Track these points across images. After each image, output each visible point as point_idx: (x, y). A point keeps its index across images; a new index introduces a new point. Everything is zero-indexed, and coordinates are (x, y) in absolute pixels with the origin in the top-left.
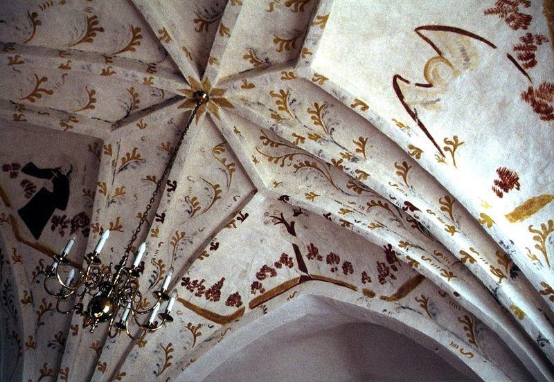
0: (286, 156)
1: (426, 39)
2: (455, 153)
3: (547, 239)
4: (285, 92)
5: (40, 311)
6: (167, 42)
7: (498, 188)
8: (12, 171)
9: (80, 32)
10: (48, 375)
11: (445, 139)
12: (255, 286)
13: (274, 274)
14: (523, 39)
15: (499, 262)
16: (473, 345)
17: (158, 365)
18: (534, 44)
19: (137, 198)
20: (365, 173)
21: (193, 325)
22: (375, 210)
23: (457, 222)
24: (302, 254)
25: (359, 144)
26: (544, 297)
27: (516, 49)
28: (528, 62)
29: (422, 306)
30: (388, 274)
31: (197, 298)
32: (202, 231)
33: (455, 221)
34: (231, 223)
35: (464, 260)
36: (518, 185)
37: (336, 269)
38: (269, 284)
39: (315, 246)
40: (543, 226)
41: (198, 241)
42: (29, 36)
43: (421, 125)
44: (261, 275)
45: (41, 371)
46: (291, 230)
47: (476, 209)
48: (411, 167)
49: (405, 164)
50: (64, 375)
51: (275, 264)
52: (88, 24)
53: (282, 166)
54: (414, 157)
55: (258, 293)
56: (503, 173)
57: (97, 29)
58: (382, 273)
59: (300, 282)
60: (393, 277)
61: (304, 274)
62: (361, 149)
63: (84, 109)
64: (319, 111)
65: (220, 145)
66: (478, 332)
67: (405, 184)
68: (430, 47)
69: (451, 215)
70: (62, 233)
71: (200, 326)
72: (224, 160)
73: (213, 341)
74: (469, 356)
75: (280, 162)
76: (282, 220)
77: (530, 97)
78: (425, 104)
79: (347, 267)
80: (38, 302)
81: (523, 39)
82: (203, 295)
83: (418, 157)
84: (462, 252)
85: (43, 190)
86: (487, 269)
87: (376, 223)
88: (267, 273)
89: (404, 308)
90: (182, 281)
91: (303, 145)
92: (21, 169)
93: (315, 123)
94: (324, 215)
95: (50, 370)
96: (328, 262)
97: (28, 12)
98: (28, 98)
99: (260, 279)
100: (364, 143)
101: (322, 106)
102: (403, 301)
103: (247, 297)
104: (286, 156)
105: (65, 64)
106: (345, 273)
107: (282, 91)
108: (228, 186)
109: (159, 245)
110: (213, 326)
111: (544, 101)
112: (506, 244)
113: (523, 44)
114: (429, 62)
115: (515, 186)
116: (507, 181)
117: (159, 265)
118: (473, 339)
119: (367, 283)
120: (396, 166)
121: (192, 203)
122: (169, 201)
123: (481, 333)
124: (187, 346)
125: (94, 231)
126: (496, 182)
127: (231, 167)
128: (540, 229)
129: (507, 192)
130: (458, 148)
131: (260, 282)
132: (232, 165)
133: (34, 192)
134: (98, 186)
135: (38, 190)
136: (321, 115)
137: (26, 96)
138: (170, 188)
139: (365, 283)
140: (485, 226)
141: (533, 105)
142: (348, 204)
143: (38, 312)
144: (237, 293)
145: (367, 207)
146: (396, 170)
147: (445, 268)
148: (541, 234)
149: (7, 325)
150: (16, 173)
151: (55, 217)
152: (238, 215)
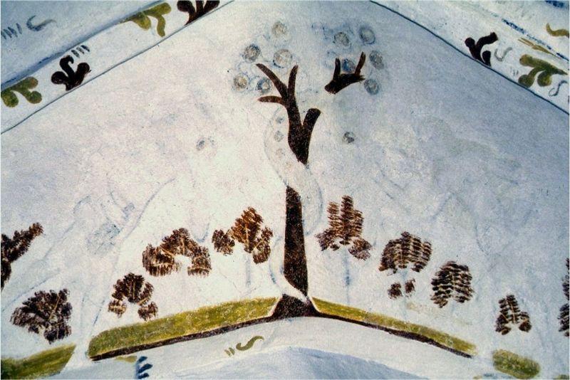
12: (130, 288)
13: (201, 265)
24: (306, 229)
32: (38, 28)
37: (410, 287)
39: (356, 206)
44: (159, 259)
46: (300, 143)
51: (215, 236)
55: (131, 315)
59: (277, 316)
61: (295, 293)
76: (287, 96)
88: (179, 258)
96: (387, 264)
99: (153, 270)
106: (440, 299)
139: (506, 331)
144: (63, 294)
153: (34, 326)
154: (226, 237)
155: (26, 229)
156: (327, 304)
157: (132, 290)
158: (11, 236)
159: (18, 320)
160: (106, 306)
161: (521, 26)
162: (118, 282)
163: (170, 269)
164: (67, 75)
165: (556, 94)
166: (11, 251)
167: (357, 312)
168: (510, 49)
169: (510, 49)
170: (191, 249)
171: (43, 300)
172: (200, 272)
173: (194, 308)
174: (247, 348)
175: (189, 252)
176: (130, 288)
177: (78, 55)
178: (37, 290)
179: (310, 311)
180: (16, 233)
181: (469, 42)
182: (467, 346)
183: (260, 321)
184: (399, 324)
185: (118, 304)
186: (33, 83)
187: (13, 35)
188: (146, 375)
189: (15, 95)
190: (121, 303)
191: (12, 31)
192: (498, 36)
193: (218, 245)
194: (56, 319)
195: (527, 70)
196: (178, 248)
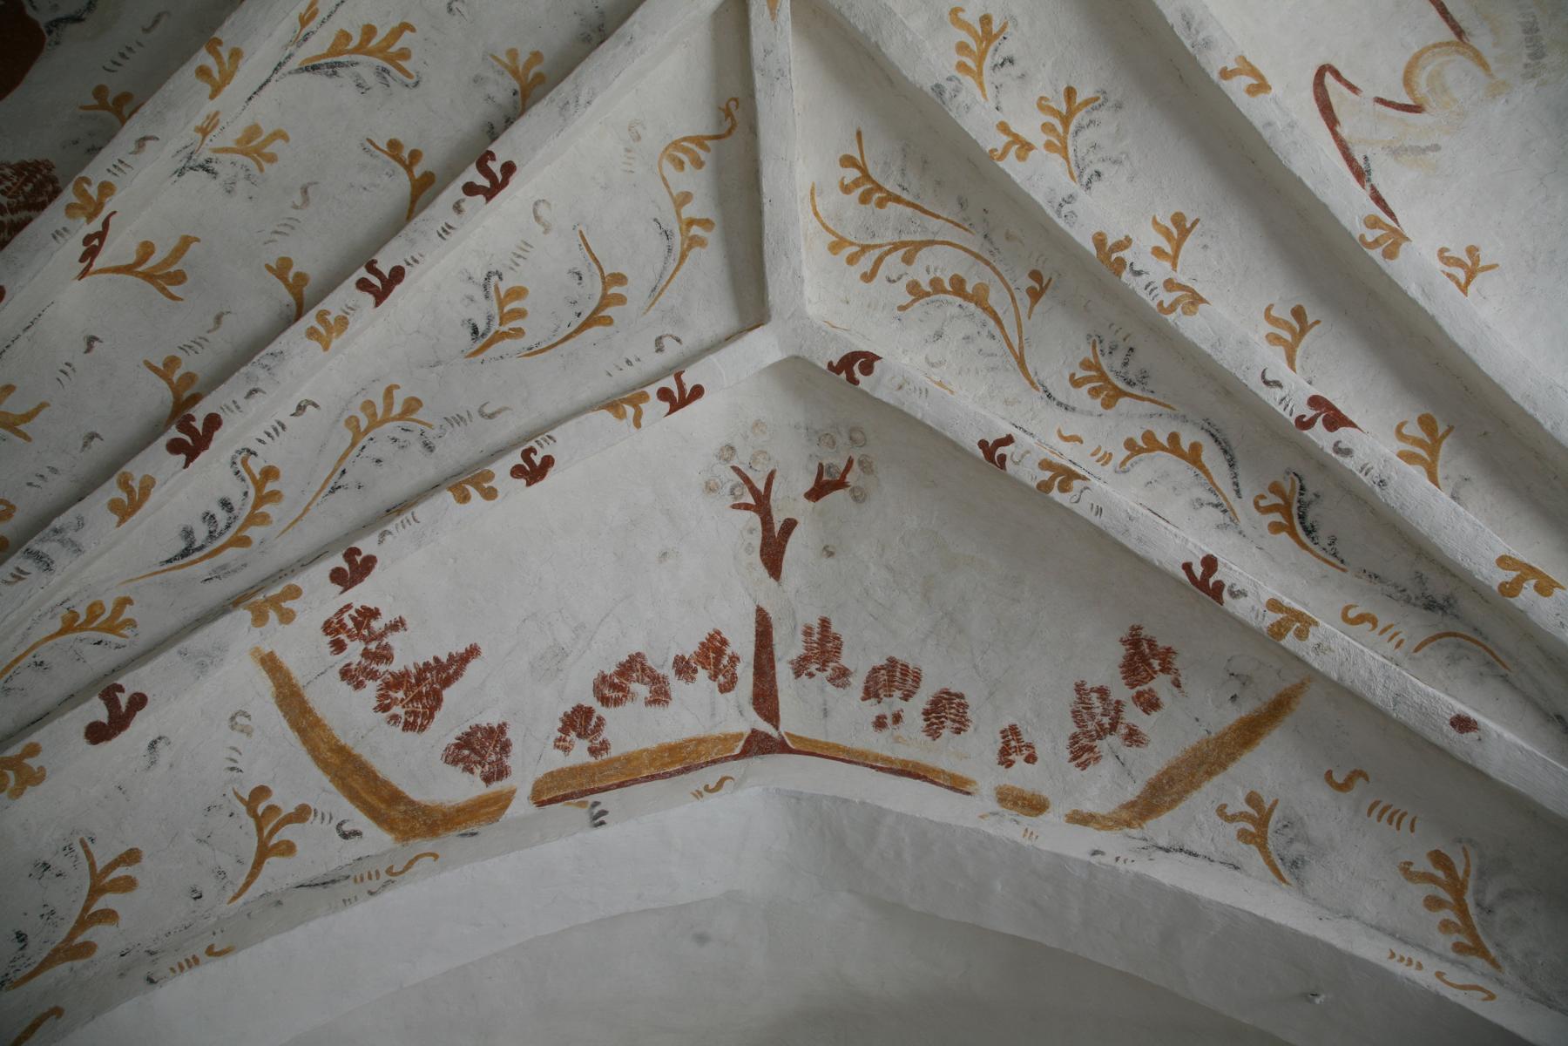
0: (896, 247)
4: (995, 29)
11: (1442, 251)
12: (579, 721)
13: (660, 696)
19: (306, 201)
20: (1193, 292)
21: (273, 800)
25: (1167, 234)
29: (1243, 836)
31: (345, 688)
32: (491, 416)
34: (629, 401)
35: (1510, 589)
37: (897, 718)
39: (835, 628)
41: (456, 450)
44: (612, 688)
46: (772, 557)
48: (1317, 322)
49: (1298, 313)
51: (676, 662)
53: (868, 277)
55: (580, 753)
58: (1091, 726)
59: (745, 753)
60: (1133, 737)
61: (765, 727)
62: (1168, 249)
65: (699, 141)
71: (302, 814)
72: (686, 198)
73: (348, 889)
75: (866, 263)
76: (762, 504)
78: (1396, 152)
82: (372, 687)
83: (1390, 254)
84: (1504, 562)
89: (1167, 851)
90: (339, 561)
91: (1020, 165)
94: (983, 444)
96: (870, 693)
99: (605, 701)
100: (1184, 233)
101: (1087, 103)
102: (1161, 827)
104: (896, 247)
106: (933, 731)
107: (986, 20)
108: (656, 292)
109: (301, 408)
110: (356, 833)
117: (259, 486)
120: (1268, 315)
121: (501, 306)
122: (447, 229)
124: (209, 887)
125: (70, 208)
127: (696, 230)
130: (1480, 277)
132: (706, 223)
134: (203, 52)
136: (1072, 128)
138: (483, 182)
139: (1010, 764)
142: (1055, 440)
144: (502, 728)
145: (1121, 453)
146: (1268, 328)
152: (670, 383)
153: (469, 766)
154: (687, 662)
155: (462, 650)
156: (801, 739)
157: (581, 725)
158: (444, 659)
159: (450, 758)
160: (551, 742)
161: (1030, 430)
162: (565, 714)
163: (624, 699)
164: (528, 468)
165: (1077, 502)
166: (444, 676)
167: (837, 747)
168: (1028, 452)
169: (1028, 452)
170: (648, 677)
171: (479, 735)
172: (659, 704)
173: (651, 744)
174: (717, 790)
175: (647, 679)
176: (578, 721)
177: (542, 446)
178: (473, 723)
179: (781, 747)
180: (451, 656)
181: (983, 444)
182: (966, 782)
183: (726, 759)
185: (564, 740)
186: (490, 476)
187: (461, 423)
188: (602, 823)
189: (467, 490)
190: (568, 738)
191: (461, 418)
192: (1014, 438)
193: (679, 672)
194: (493, 758)
195: (1047, 475)
196: (634, 675)
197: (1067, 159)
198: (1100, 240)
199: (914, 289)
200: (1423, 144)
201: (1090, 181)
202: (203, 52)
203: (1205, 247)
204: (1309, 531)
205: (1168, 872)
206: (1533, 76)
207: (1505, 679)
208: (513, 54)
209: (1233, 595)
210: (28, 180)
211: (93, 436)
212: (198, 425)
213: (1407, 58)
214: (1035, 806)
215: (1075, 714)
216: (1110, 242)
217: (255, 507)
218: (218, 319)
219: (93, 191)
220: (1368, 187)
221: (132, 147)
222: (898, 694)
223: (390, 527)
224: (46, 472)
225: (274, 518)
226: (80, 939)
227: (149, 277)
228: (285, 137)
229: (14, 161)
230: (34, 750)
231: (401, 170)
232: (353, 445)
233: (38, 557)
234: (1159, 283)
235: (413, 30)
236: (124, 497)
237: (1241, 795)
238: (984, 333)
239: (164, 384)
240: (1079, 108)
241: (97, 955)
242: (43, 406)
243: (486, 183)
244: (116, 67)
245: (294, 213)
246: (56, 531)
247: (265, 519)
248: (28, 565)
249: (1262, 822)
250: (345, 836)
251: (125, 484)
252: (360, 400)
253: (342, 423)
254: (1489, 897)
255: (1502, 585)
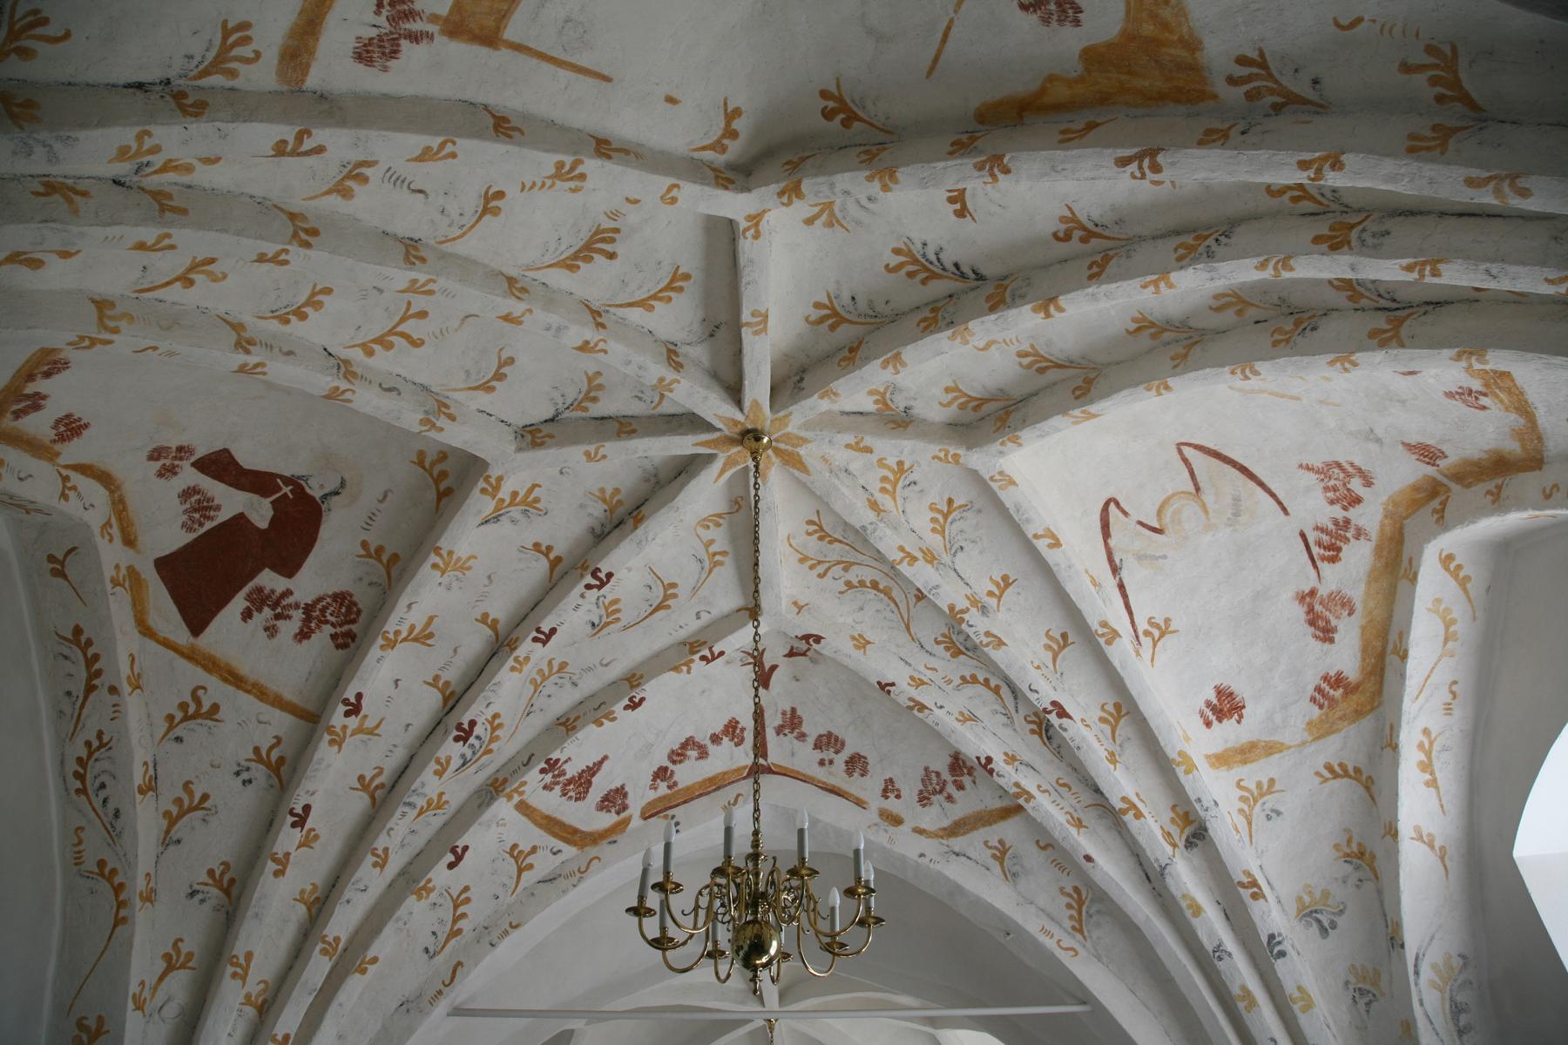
0: (839, 563)
1: (1185, 461)
2: (1160, 644)
3: (1259, 804)
4: (906, 466)
5: (175, 810)
6: (756, 333)
7: (1209, 714)
8: (168, 462)
9: (563, 248)
10: (183, 966)
11: (1150, 618)
12: (661, 774)
13: (703, 754)
14: (1336, 522)
15: (1173, 820)
16: (1078, 936)
17: (434, 933)
18: (1349, 535)
20: (1000, 639)
22: (970, 690)
23: (1120, 746)
24: (767, 722)
25: (998, 585)
26: (1242, 890)
27: (1317, 528)
28: (1327, 553)
29: (994, 856)
30: (941, 792)
32: (606, 665)
33: (1118, 742)
34: (684, 664)
35: (1125, 812)
36: (1241, 716)
37: (831, 762)
38: (689, 773)
40: (1259, 785)
41: (590, 684)
42: (459, 232)
43: (1121, 587)
44: (677, 756)
45: (167, 957)
47: (1172, 745)
49: (1064, 636)
50: (239, 970)
52: (591, 237)
53: (821, 576)
54: (1102, 641)
55: (663, 788)
56: (1224, 694)
57: (601, 251)
58: (930, 788)
60: (949, 798)
62: (997, 592)
63: (470, 389)
64: (949, 512)
65: (719, 516)
66: (1091, 916)
67: (1051, 666)
68: (1186, 474)
69: (1113, 732)
70: (271, 631)
71: (534, 850)
72: (711, 542)
73: (561, 883)
74: (1072, 953)
75: (821, 569)
77: (1308, 599)
78: (1140, 558)
79: (856, 764)
80: (170, 791)
81: (1336, 522)
82: (558, 789)
83: (1109, 642)
84: (1124, 799)
85: (240, 518)
86: (1159, 833)
87: (966, 712)
89: (958, 855)
92: (193, 459)
93: (934, 530)
94: (879, 683)
95: (190, 955)
96: (818, 746)
97: (489, 188)
98: (363, 346)
99: (674, 762)
100: (1008, 585)
101: (960, 507)
102: (957, 843)
103: (637, 797)
104: (839, 563)
105: (516, 314)
106: (850, 773)
108: (695, 590)
110: (559, 851)
111: (1328, 613)
112: (1205, 804)
113: (1331, 527)
114: (1173, 495)
115: (1236, 716)
116: (1225, 706)
118: (1081, 926)
119: (892, 796)
121: (606, 609)
122: (578, 606)
123: (1095, 918)
124: (500, 893)
125: (382, 647)
126: (1208, 704)
127: (717, 558)
128: (1253, 786)
129: (1220, 721)
130: (1167, 636)
131: (671, 767)
132: (724, 553)
133: (210, 518)
134: (433, 555)
135: (223, 516)
136: (950, 520)
137: (360, 342)
139: (887, 798)
140: (1180, 771)
141: (1308, 613)
142: (922, 668)
143: (167, 814)
144: (623, 787)
146: (1046, 641)
147: (1072, 811)
148: (1252, 795)
149: (80, 842)
150: (174, 467)
151: (260, 590)
152: (706, 652)
155: (599, 759)
156: (780, 766)
158: (591, 765)
161: (909, 661)
167: (798, 772)
173: (700, 779)
182: (864, 802)
183: (739, 780)
184: (824, 783)
195: (912, 704)
197: (944, 537)
198: (952, 608)
199: (849, 584)
200: (1157, 555)
201: (956, 552)
202: (433, 555)
203: (1019, 594)
204: (1049, 738)
205: (955, 871)
206: (1231, 525)
207: (1120, 833)
208: (602, 490)
209: (998, 775)
210: (341, 605)
211: (408, 725)
212: (466, 726)
213: (1164, 497)
214: (896, 821)
215: (923, 780)
216: (957, 609)
217: (492, 734)
218: (455, 651)
219: (391, 636)
220: (1117, 578)
221: (406, 610)
222: (832, 750)
223: (566, 745)
224: (391, 748)
225: (502, 736)
226: (455, 928)
227: (416, 640)
228: (475, 557)
229: (330, 593)
230: (429, 881)
231: (542, 556)
232: (535, 692)
233: (409, 804)
234: (982, 632)
235: (540, 486)
236: (439, 767)
237: (996, 839)
238: (888, 609)
239: (435, 690)
240: (955, 510)
241: (464, 933)
242: (382, 720)
243: (598, 583)
244: (369, 527)
245: (486, 589)
246: (414, 791)
247: (498, 738)
248: (406, 809)
249: (1004, 852)
250: (555, 854)
251: (438, 762)
252: (536, 670)
253: (528, 683)
254: (1091, 912)
255: (1120, 809)
